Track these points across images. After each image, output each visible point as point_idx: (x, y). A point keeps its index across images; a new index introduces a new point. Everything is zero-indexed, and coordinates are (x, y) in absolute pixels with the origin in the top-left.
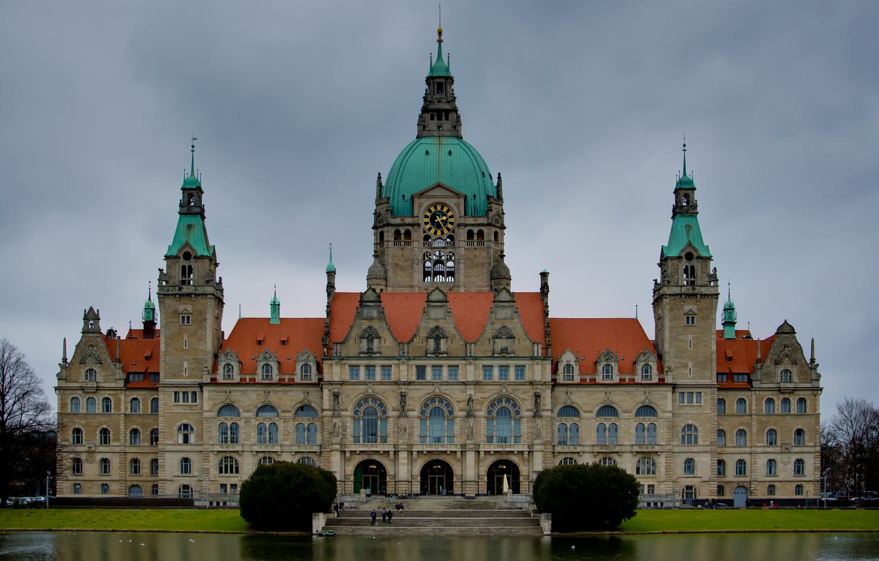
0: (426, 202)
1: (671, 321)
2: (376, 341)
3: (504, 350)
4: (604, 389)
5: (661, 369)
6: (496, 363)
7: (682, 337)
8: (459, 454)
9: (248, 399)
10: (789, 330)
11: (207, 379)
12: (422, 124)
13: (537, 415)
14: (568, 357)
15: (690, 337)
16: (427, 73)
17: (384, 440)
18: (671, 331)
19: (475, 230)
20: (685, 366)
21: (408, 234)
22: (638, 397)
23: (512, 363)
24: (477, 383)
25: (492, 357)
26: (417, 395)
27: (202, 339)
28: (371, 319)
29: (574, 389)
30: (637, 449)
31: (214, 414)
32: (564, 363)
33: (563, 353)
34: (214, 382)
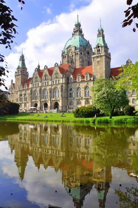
5: (90, 77)
6: (55, 80)
7: (97, 68)
9: (23, 93)
11: (18, 90)
12: (73, 35)
16: (75, 24)
18: (94, 67)
19: (77, 53)
21: (66, 56)
22: (85, 84)
24: (51, 85)
25: (55, 79)
26: (43, 88)
27: (19, 83)
28: (36, 74)
29: (72, 84)
31: (19, 96)
34: (19, 91)
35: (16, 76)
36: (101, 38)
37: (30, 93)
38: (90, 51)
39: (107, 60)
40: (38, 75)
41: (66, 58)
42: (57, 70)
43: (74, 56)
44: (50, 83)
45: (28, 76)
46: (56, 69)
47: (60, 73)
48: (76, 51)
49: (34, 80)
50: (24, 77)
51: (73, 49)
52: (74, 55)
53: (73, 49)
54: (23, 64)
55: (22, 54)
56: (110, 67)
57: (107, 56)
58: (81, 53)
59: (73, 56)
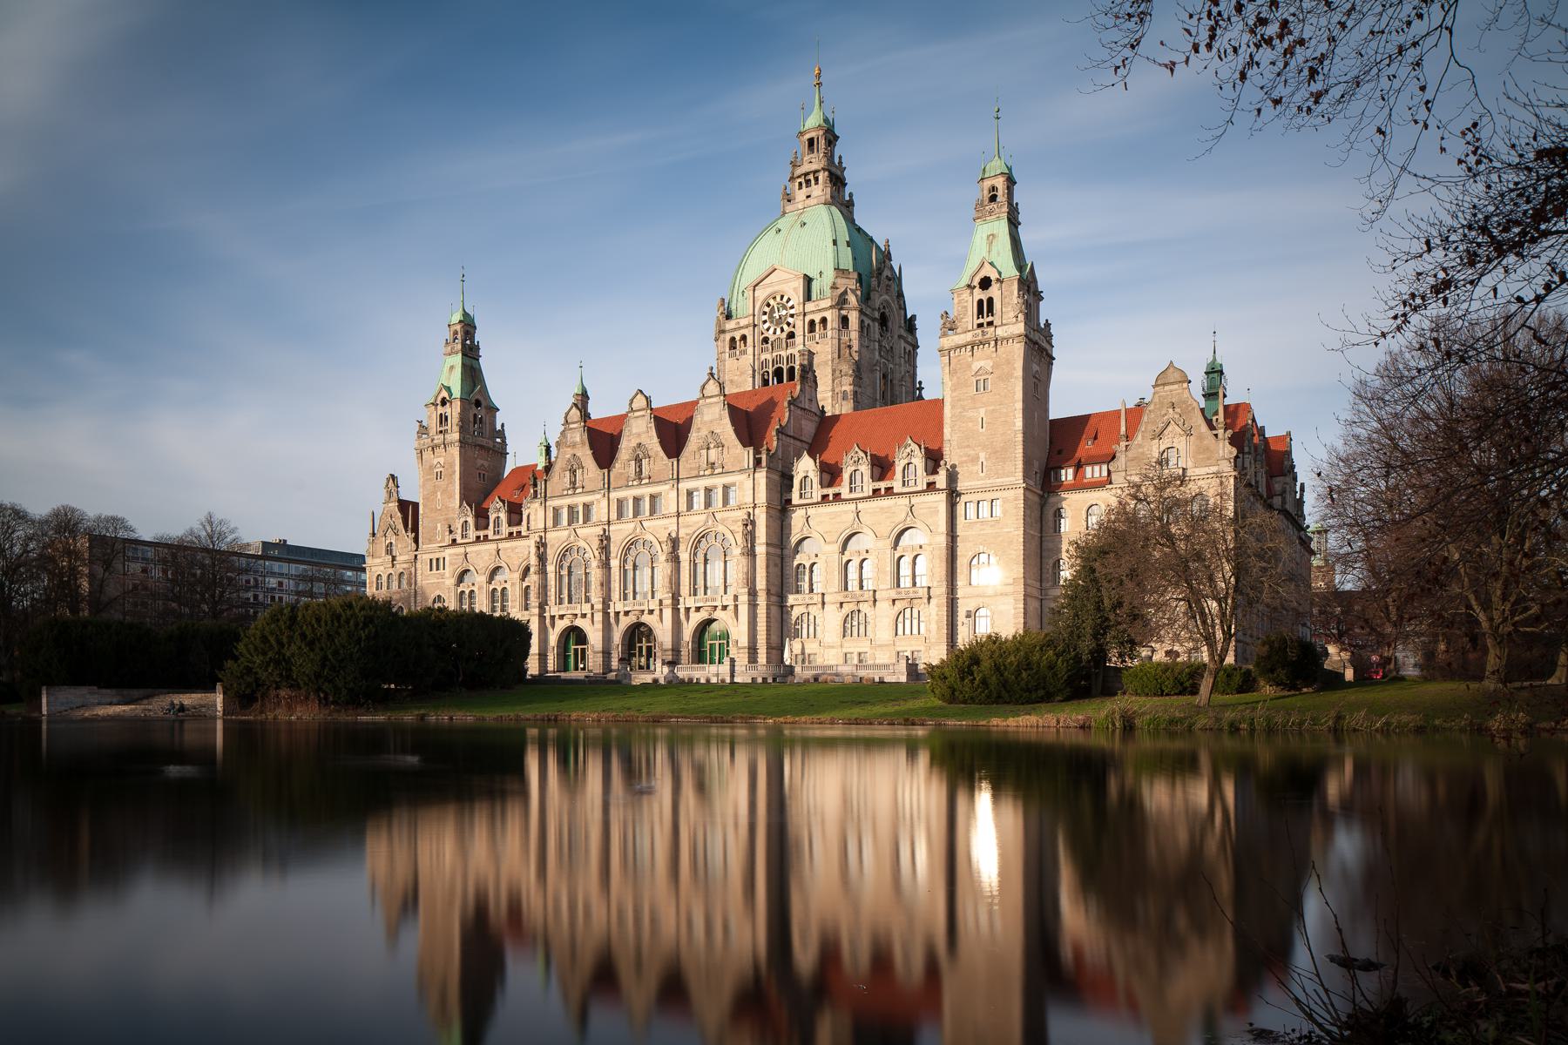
0: (761, 294)
1: (953, 391)
2: (579, 473)
3: (712, 465)
4: (852, 506)
7: (970, 414)
8: (657, 612)
10: (1177, 376)
13: (751, 553)
14: (805, 467)
15: (982, 412)
17: (588, 600)
19: (817, 321)
20: (975, 459)
23: (718, 482)
28: (574, 445)
30: (893, 594)
32: (801, 475)
33: (799, 457)
35: (427, 455)
36: (1002, 228)
37: (533, 560)
38: (895, 306)
39: (1036, 367)
40: (589, 452)
41: (750, 350)
42: (713, 420)
43: (799, 339)
44: (670, 500)
45: (502, 453)
46: (706, 418)
47: (737, 442)
48: (810, 306)
49: (559, 480)
50: (480, 462)
51: (795, 289)
52: (799, 332)
53: (795, 292)
54: (472, 374)
55: (465, 314)
56: (1046, 411)
57: (1036, 343)
58: (844, 321)
59: (791, 335)
